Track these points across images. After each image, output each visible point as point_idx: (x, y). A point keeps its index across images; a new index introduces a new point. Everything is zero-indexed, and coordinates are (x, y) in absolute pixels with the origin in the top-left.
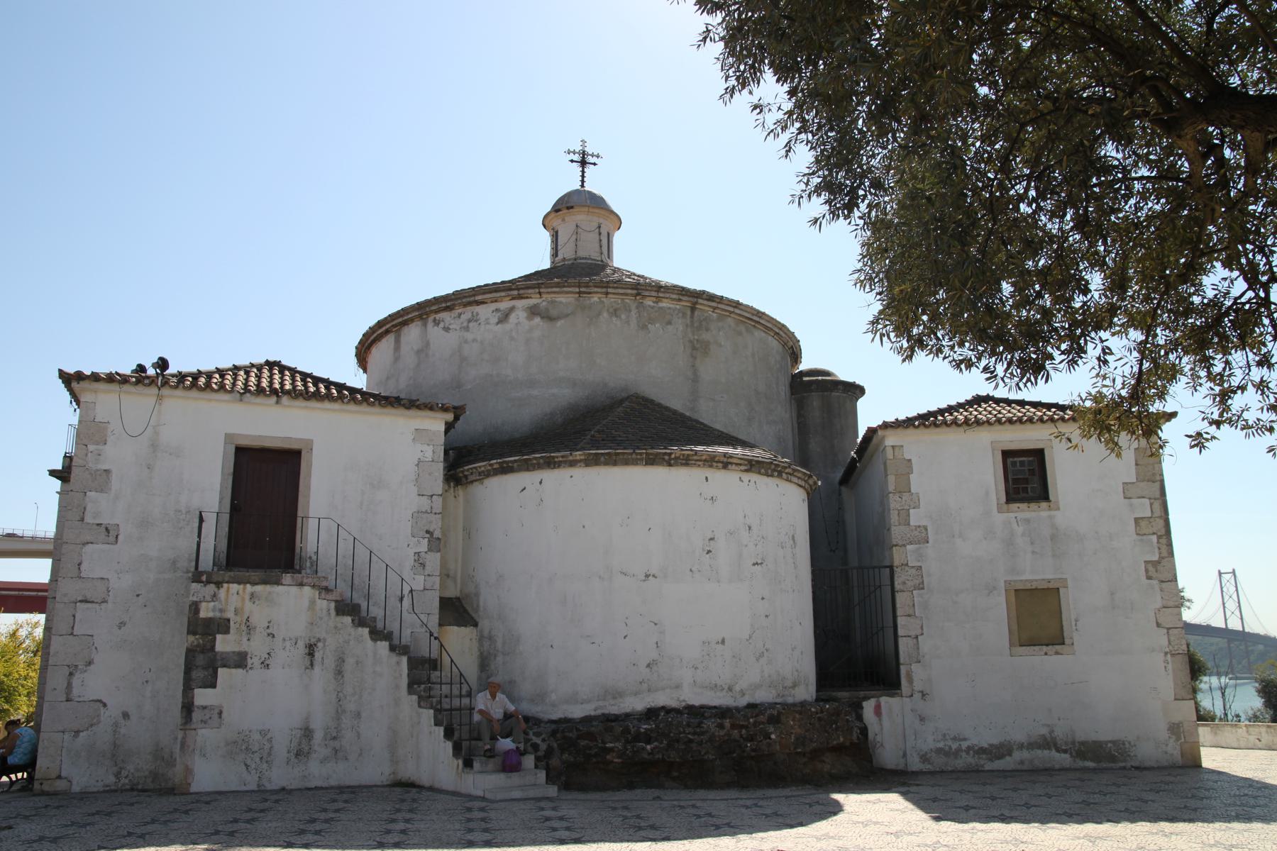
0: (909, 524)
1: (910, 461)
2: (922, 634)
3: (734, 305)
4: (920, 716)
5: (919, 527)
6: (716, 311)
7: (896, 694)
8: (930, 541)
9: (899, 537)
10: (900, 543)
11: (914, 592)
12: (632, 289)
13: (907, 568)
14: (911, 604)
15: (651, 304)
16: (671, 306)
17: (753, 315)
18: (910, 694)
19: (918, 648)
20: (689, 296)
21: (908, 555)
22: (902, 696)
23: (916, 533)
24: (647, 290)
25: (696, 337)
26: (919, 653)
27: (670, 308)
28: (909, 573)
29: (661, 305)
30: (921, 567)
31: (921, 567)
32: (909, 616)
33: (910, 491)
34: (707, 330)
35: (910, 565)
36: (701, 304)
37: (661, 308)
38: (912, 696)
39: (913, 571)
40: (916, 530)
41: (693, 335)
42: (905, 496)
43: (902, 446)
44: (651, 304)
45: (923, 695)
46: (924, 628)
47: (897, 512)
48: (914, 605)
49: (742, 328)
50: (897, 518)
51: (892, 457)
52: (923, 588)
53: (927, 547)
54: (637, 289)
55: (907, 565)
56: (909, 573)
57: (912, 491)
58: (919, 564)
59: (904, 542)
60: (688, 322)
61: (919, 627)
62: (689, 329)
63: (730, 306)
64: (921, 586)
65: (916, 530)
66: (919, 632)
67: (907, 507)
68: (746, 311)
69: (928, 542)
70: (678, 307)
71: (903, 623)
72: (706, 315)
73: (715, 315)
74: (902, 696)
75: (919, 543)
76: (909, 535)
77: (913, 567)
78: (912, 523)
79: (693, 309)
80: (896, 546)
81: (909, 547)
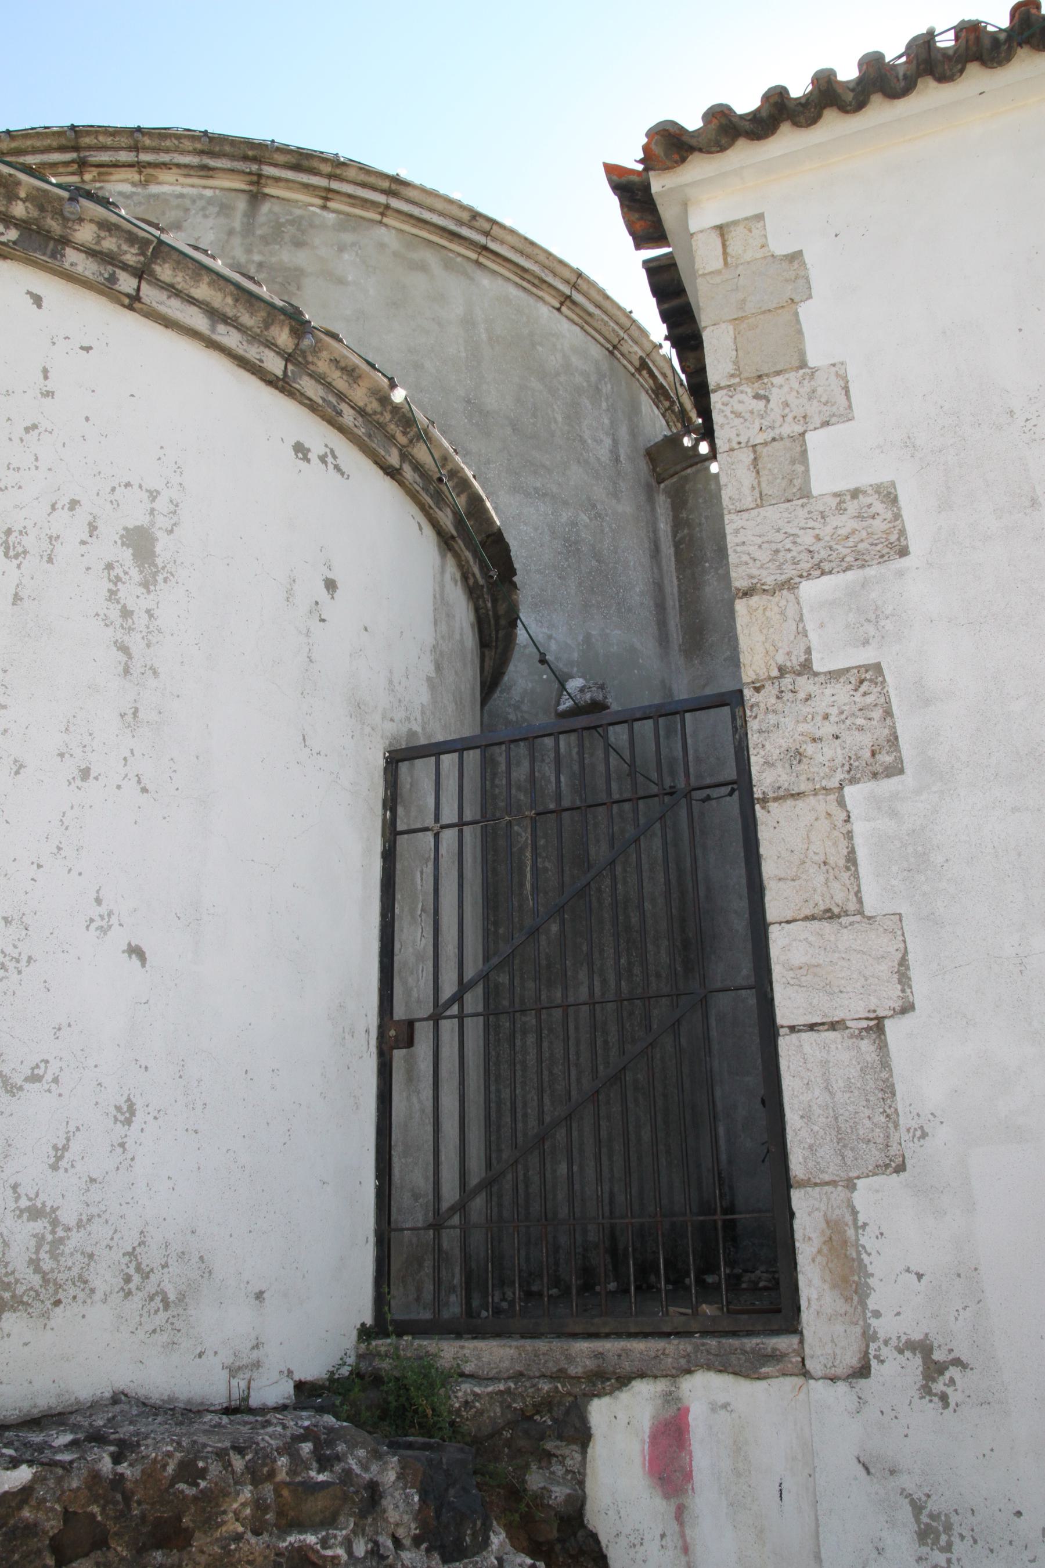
0: (805, 493)
1: (796, 257)
2: (907, 1008)
3: (386, 184)
4: (917, 1508)
5: (855, 493)
6: (331, 204)
7: (775, 1357)
8: (916, 543)
9: (764, 556)
10: (770, 580)
11: (851, 792)
12: (62, 149)
13: (805, 685)
14: (838, 858)
15: (127, 188)
16: (186, 190)
17: (460, 222)
18: (850, 1359)
19: (889, 1090)
20: (232, 157)
21: (810, 626)
22: (806, 1374)
23: (845, 523)
24: (104, 148)
25: (257, 258)
26: (892, 1118)
27: (181, 196)
28: (821, 705)
29: (154, 189)
30: (878, 668)
31: (878, 668)
32: (830, 915)
33: (803, 364)
34: (298, 244)
35: (817, 667)
36: (277, 180)
37: (156, 196)
38: (863, 1371)
39: (841, 693)
40: (840, 509)
41: (249, 251)
42: (781, 389)
43: (760, 217)
44: (127, 188)
45: (933, 1370)
46: (916, 974)
47: (746, 457)
48: (851, 859)
49: (430, 257)
50: (747, 478)
51: (719, 264)
52: (896, 769)
53: (900, 573)
54: (76, 149)
55: (806, 667)
56: (821, 705)
57: (812, 362)
58: (866, 656)
59: (790, 571)
60: (237, 224)
61: (885, 969)
62: (237, 241)
63: (374, 188)
64: (886, 758)
65: (840, 509)
66: (888, 996)
67: (790, 428)
68: (432, 210)
69: (904, 552)
70: (208, 193)
71: (798, 956)
72: (298, 212)
73: (332, 216)
74: (806, 1374)
75: (861, 561)
76: (807, 539)
77: (835, 675)
78: (817, 487)
79: (256, 198)
80: (747, 593)
81: (810, 590)
